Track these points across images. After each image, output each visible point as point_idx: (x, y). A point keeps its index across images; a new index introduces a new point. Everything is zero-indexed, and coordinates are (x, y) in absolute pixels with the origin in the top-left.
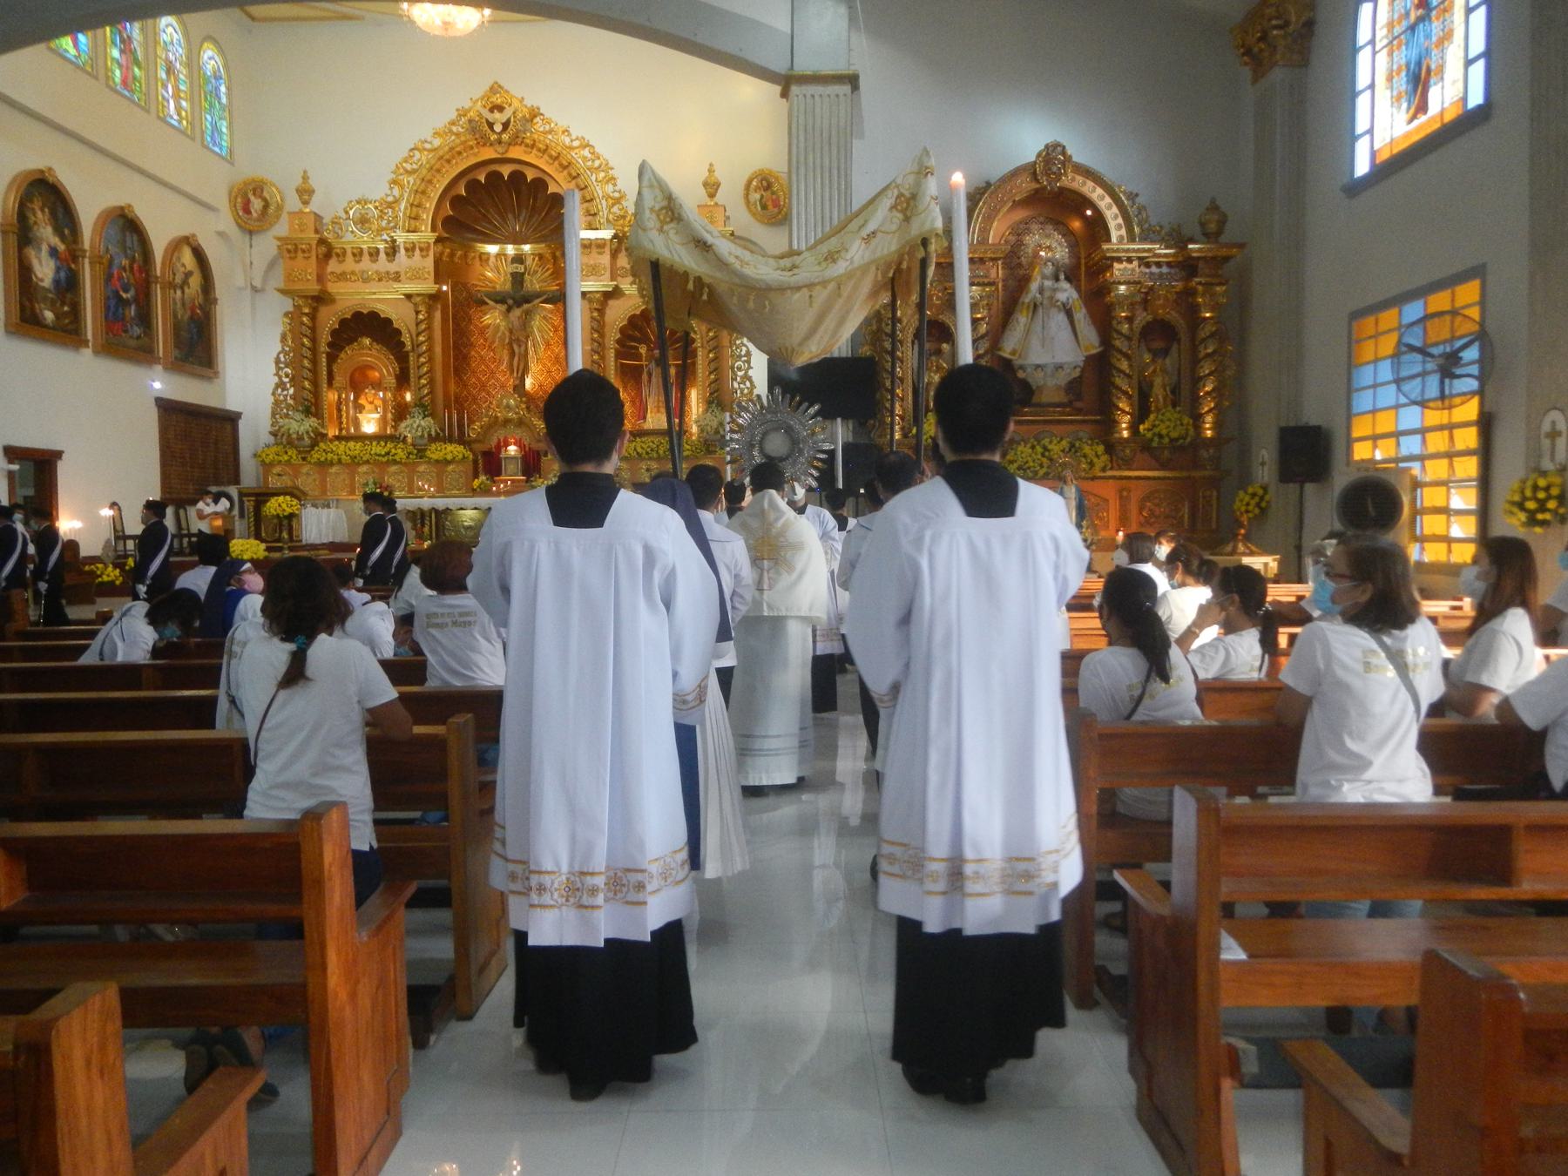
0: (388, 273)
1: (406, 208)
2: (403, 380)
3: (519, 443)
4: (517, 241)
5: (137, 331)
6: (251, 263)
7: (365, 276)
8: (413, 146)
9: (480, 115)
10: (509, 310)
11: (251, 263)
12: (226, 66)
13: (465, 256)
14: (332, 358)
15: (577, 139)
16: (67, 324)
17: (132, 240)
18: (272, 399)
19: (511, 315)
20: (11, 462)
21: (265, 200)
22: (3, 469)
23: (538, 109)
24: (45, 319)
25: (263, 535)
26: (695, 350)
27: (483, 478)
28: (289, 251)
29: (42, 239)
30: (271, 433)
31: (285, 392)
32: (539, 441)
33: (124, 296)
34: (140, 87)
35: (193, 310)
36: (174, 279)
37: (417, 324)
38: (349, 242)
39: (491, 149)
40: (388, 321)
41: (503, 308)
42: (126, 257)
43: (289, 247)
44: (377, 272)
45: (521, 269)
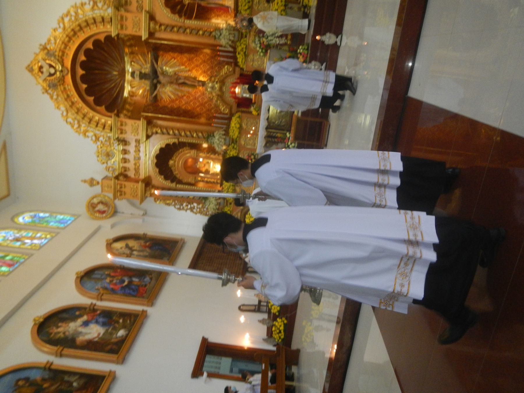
0: (136, 146)
1: (99, 130)
2: (195, 147)
3: (235, 85)
4: (123, 73)
5: (147, 279)
7: (137, 158)
8: (65, 122)
9: (45, 80)
10: (159, 82)
11: (132, 214)
12: (31, 211)
13: (130, 104)
14: (180, 182)
15: (59, 24)
16: (130, 321)
17: (97, 275)
18: (199, 215)
20: (202, 374)
21: (99, 203)
22: (206, 381)
23: (41, 45)
24: (122, 336)
27: (252, 109)
28: (121, 195)
29: (76, 330)
31: (196, 208)
33: (126, 283)
34: (17, 257)
35: (146, 247)
37: (163, 133)
38: (119, 164)
39: (66, 77)
40: (161, 150)
41: (159, 86)
42: (106, 278)
43: (119, 194)
44: (135, 151)
45: (137, 73)
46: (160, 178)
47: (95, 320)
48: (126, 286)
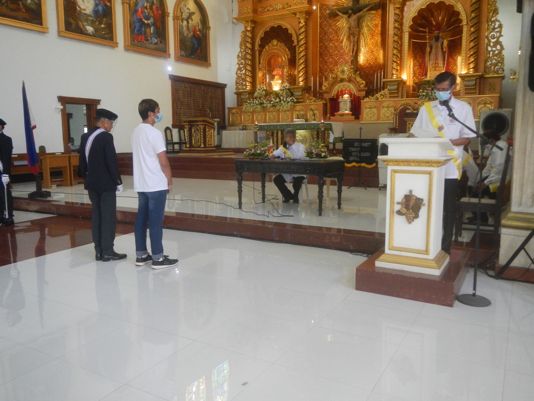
2: (292, 62)
6: (233, 10)
14: (260, 54)
16: (104, 34)
18: (235, 76)
19: (350, 19)
24: (87, 31)
25: (193, 143)
26: (463, 26)
30: (235, 93)
31: (241, 72)
32: (360, 91)
33: (146, 22)
35: (194, 31)
36: (182, 16)
40: (287, 29)
46: (262, 33)
47: (99, 3)
48: (144, 22)
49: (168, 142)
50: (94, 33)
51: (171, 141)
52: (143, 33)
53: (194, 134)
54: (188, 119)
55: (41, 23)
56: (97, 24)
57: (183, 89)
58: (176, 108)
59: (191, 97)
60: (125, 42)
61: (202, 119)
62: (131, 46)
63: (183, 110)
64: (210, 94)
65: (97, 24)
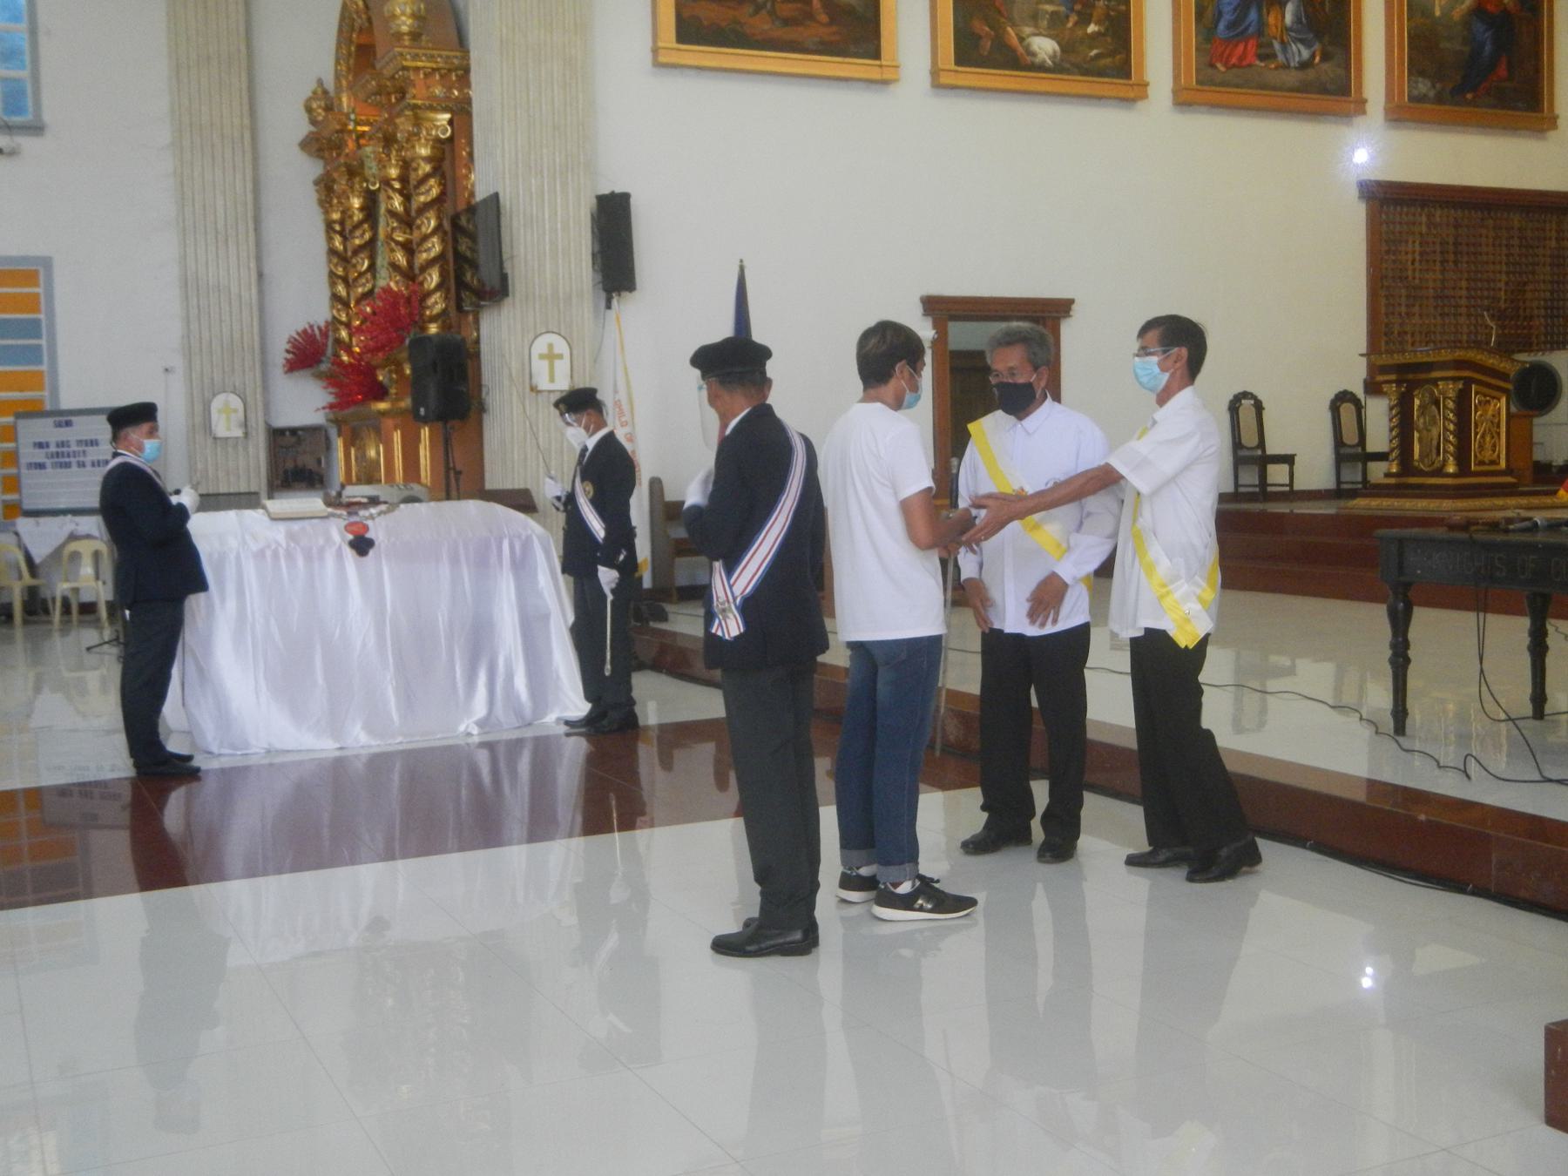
16: (1097, 56)
24: (1034, 54)
25: (1416, 456)
49: (1343, 451)
50: (1057, 60)
51: (1359, 450)
52: (1251, 30)
53: (1418, 417)
54: (1399, 359)
55: (876, 55)
56: (1070, 25)
57: (1421, 234)
58: (1386, 314)
59: (1456, 262)
60: (1176, 77)
61: (1450, 357)
62: (1199, 87)
63: (1416, 320)
64: (1553, 243)
65: (1070, 25)
